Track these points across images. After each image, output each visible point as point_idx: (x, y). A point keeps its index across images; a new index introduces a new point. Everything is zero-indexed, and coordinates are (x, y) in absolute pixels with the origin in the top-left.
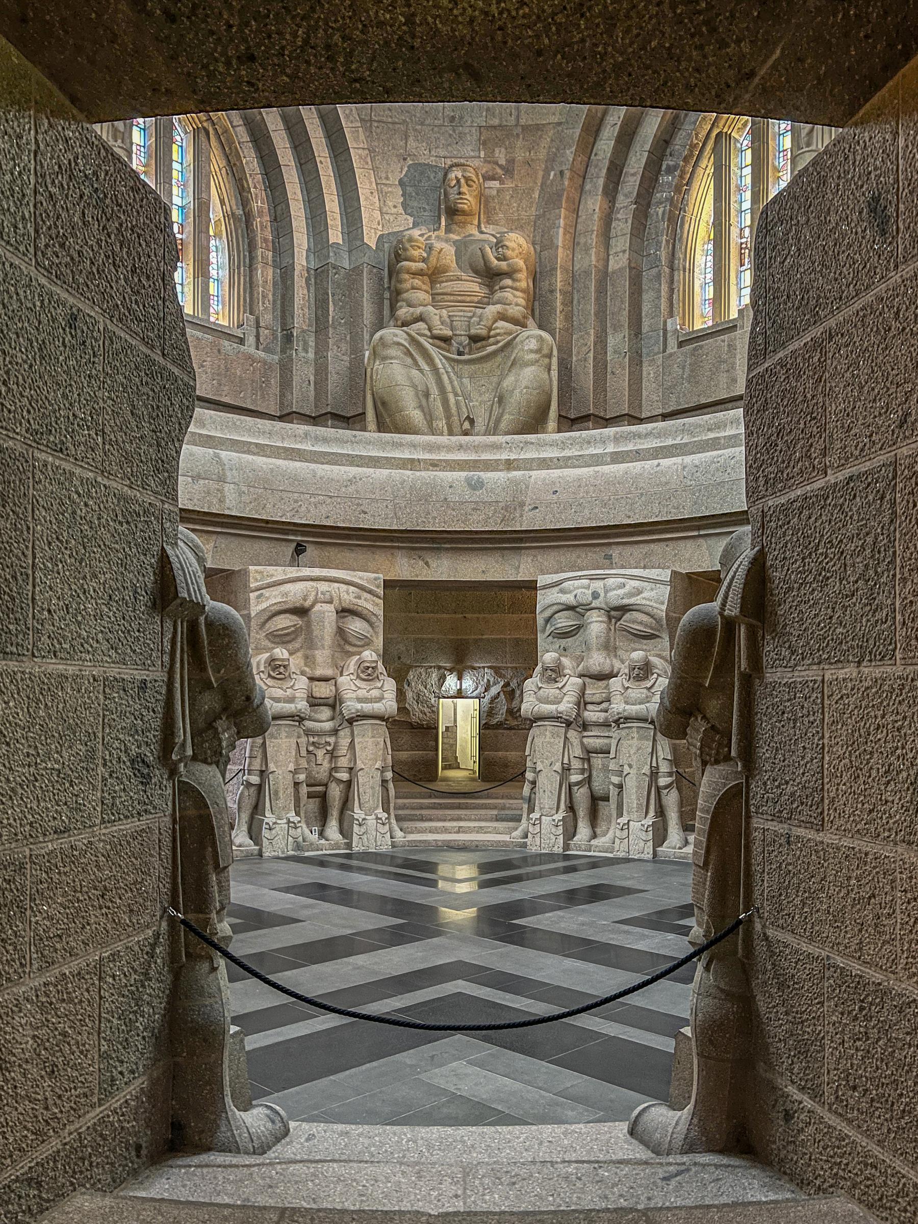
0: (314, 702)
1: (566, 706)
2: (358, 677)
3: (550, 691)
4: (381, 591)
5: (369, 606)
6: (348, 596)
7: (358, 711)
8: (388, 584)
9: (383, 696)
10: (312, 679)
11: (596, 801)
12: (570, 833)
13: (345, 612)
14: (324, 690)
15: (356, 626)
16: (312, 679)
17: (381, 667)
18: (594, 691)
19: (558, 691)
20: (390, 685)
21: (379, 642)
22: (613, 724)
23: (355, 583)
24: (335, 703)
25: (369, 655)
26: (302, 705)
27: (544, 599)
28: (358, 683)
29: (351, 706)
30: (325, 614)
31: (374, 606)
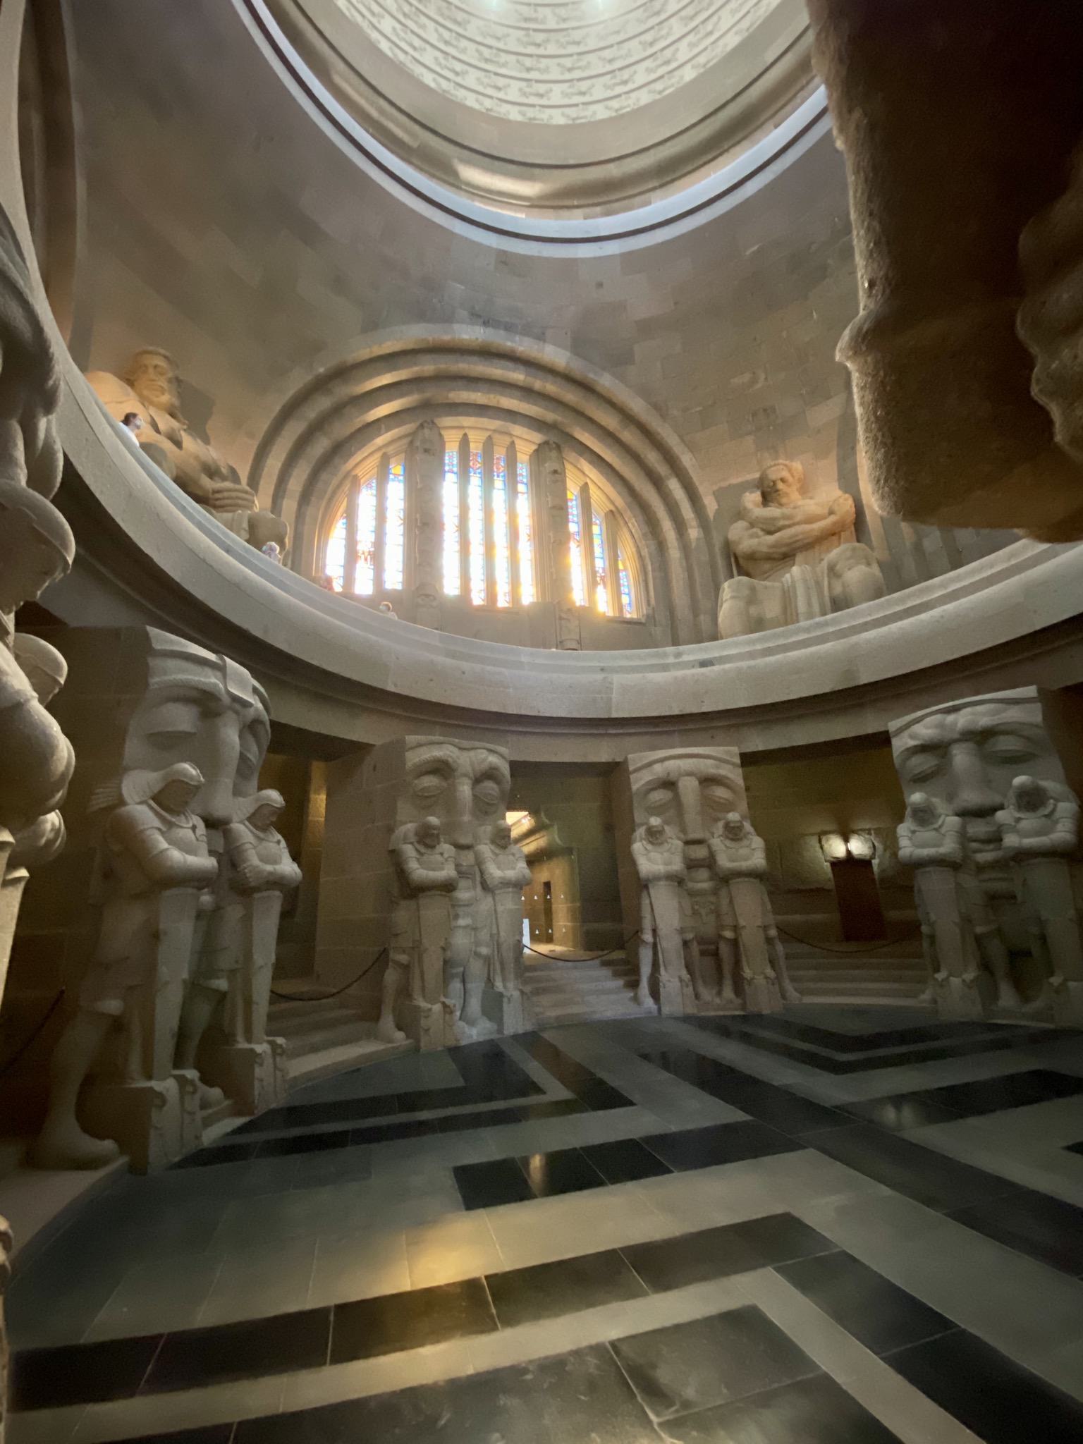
0: (691, 865)
1: (948, 846)
2: (727, 838)
3: (927, 834)
4: (738, 761)
5: (730, 775)
6: (709, 767)
7: (729, 869)
8: (744, 757)
9: (752, 853)
10: (687, 843)
11: (1017, 956)
12: (991, 995)
13: (708, 781)
14: (700, 852)
15: (720, 793)
16: (687, 843)
17: (748, 826)
18: (979, 828)
19: (934, 833)
20: (758, 842)
21: (743, 806)
22: (1012, 863)
23: (718, 757)
24: (710, 863)
25: (733, 816)
26: (677, 866)
27: (900, 744)
28: (728, 843)
29: (724, 862)
30: (689, 788)
31: (736, 775)
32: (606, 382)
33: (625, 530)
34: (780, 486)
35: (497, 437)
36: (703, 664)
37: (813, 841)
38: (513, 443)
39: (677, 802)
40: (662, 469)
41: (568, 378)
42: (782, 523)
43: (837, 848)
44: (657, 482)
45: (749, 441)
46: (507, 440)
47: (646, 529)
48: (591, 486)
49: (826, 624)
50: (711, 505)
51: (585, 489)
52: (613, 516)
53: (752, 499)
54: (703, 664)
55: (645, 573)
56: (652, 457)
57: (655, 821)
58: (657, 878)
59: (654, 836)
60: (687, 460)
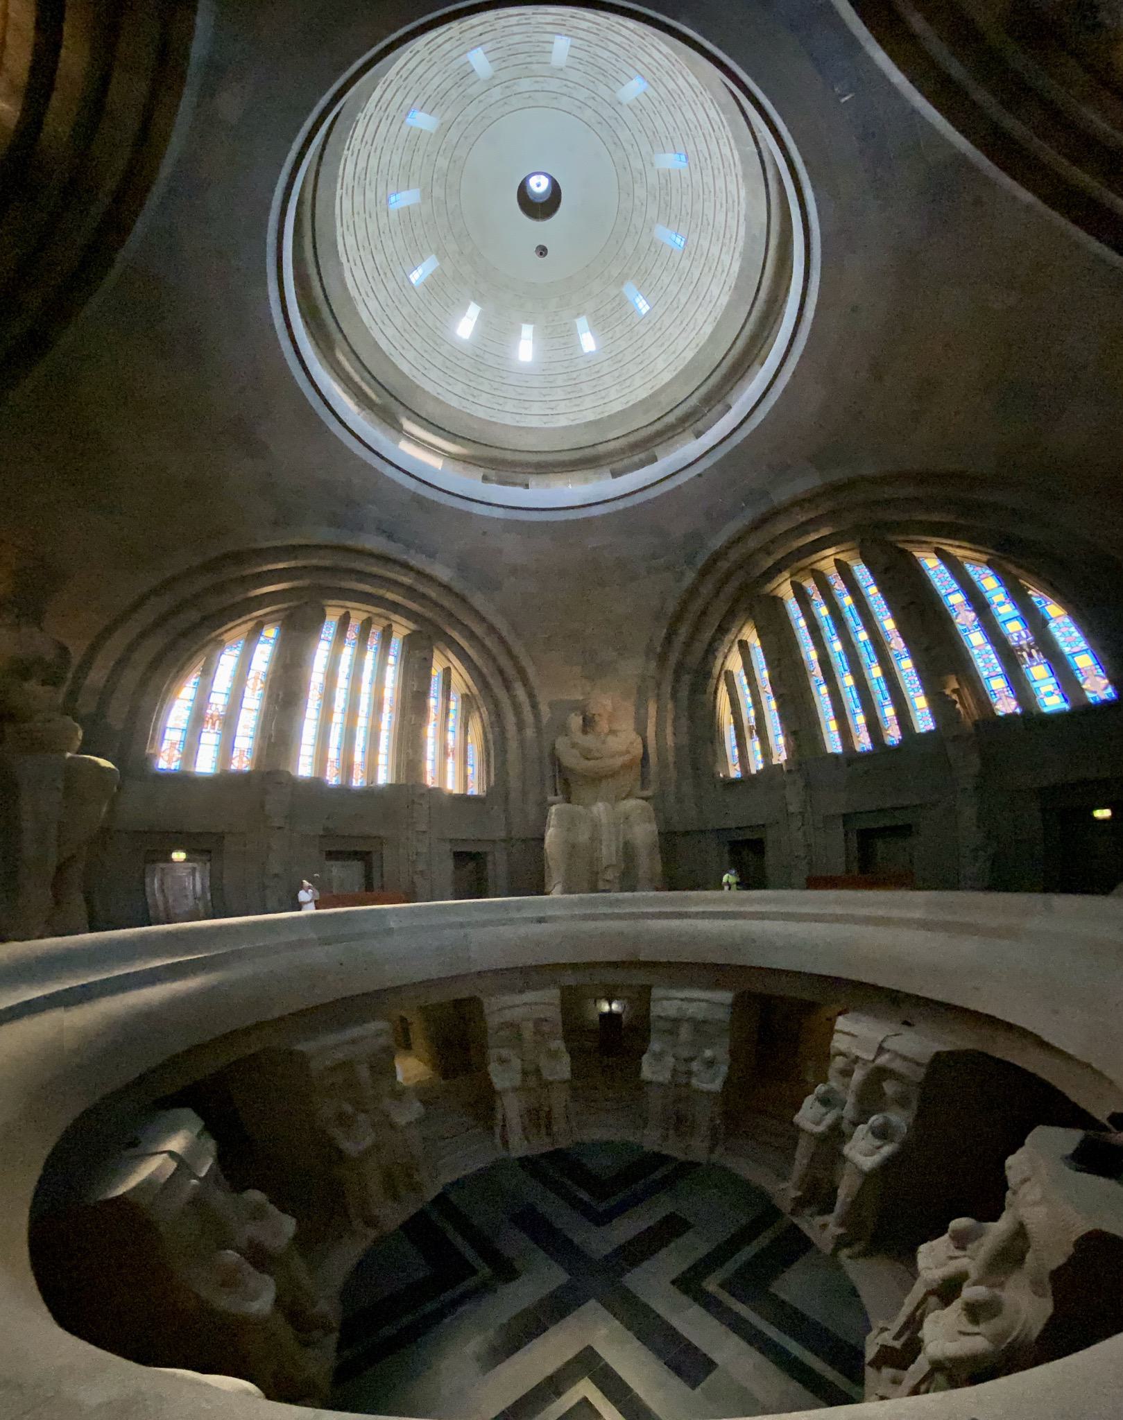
0: (525, 1073)
24: (538, 1071)
29: (547, 1075)
32: (478, 600)
33: (477, 714)
34: (597, 718)
35: (376, 619)
36: (541, 920)
37: (591, 1001)
38: (390, 626)
39: (519, 1036)
40: (511, 672)
41: (447, 588)
42: (597, 755)
43: (605, 1007)
44: (508, 686)
45: (577, 670)
46: (386, 623)
47: (493, 718)
48: (453, 671)
49: (618, 902)
50: (544, 709)
51: (447, 672)
52: (467, 699)
53: (576, 721)
54: (541, 920)
55: (488, 755)
56: (504, 661)
57: (505, 1052)
58: (506, 1090)
59: (503, 1061)
60: (531, 671)
